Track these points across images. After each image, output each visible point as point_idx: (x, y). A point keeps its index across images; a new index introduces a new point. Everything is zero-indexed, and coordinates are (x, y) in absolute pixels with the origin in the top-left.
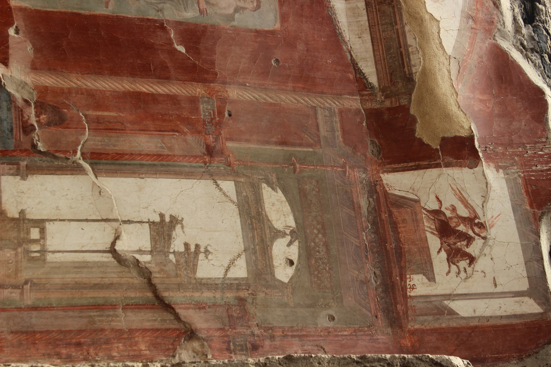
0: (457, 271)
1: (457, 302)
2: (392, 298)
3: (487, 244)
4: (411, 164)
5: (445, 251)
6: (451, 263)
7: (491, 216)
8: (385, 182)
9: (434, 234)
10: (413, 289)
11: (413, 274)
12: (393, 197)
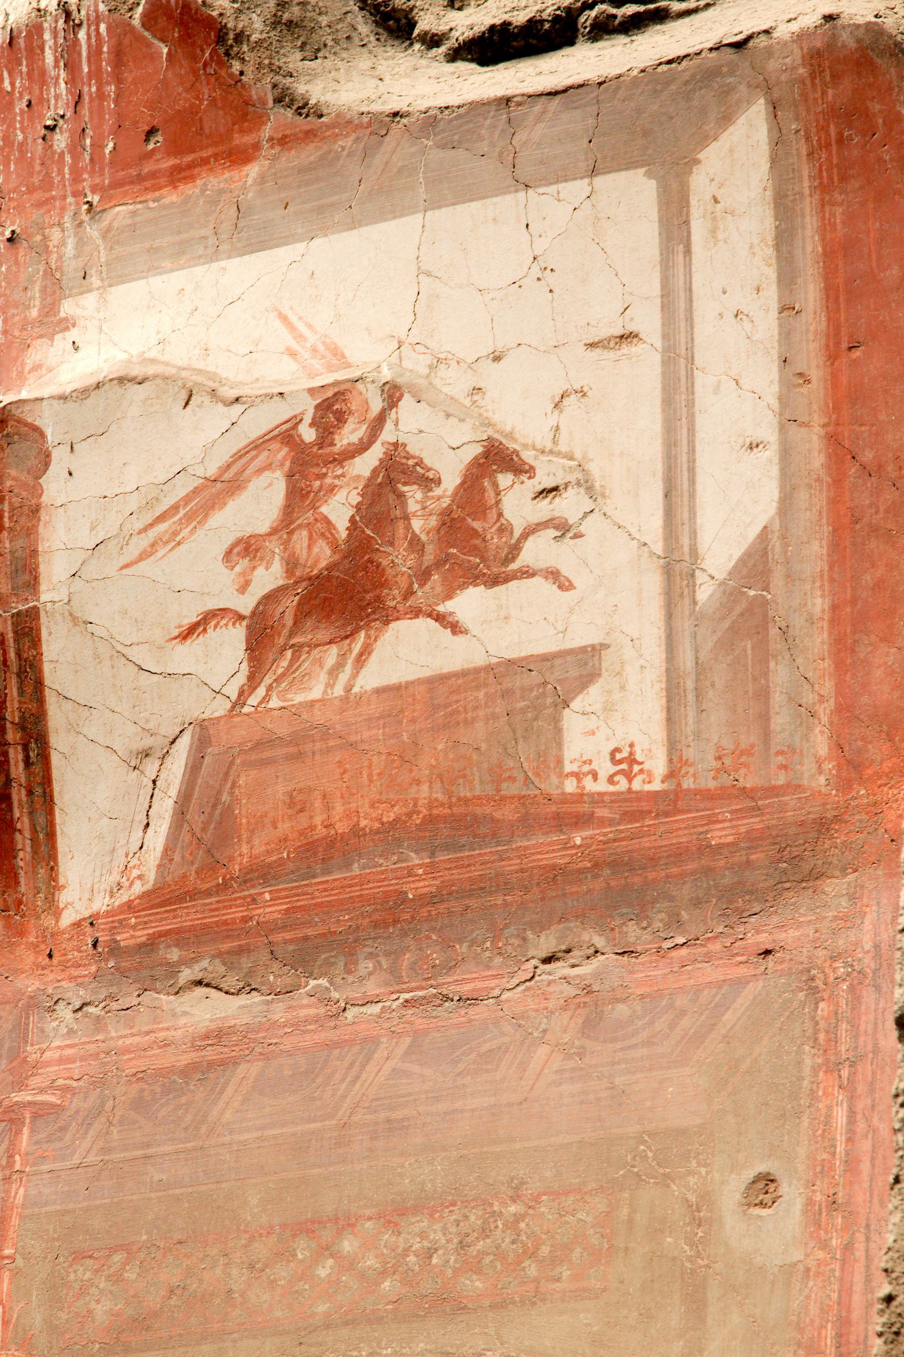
0: (552, 533)
1: (705, 540)
2: (675, 870)
3: (422, 382)
4: (17, 770)
5: (449, 596)
6: (514, 566)
7: (286, 358)
8: (101, 904)
9: (366, 651)
10: (631, 760)
11: (559, 762)
12: (177, 858)
